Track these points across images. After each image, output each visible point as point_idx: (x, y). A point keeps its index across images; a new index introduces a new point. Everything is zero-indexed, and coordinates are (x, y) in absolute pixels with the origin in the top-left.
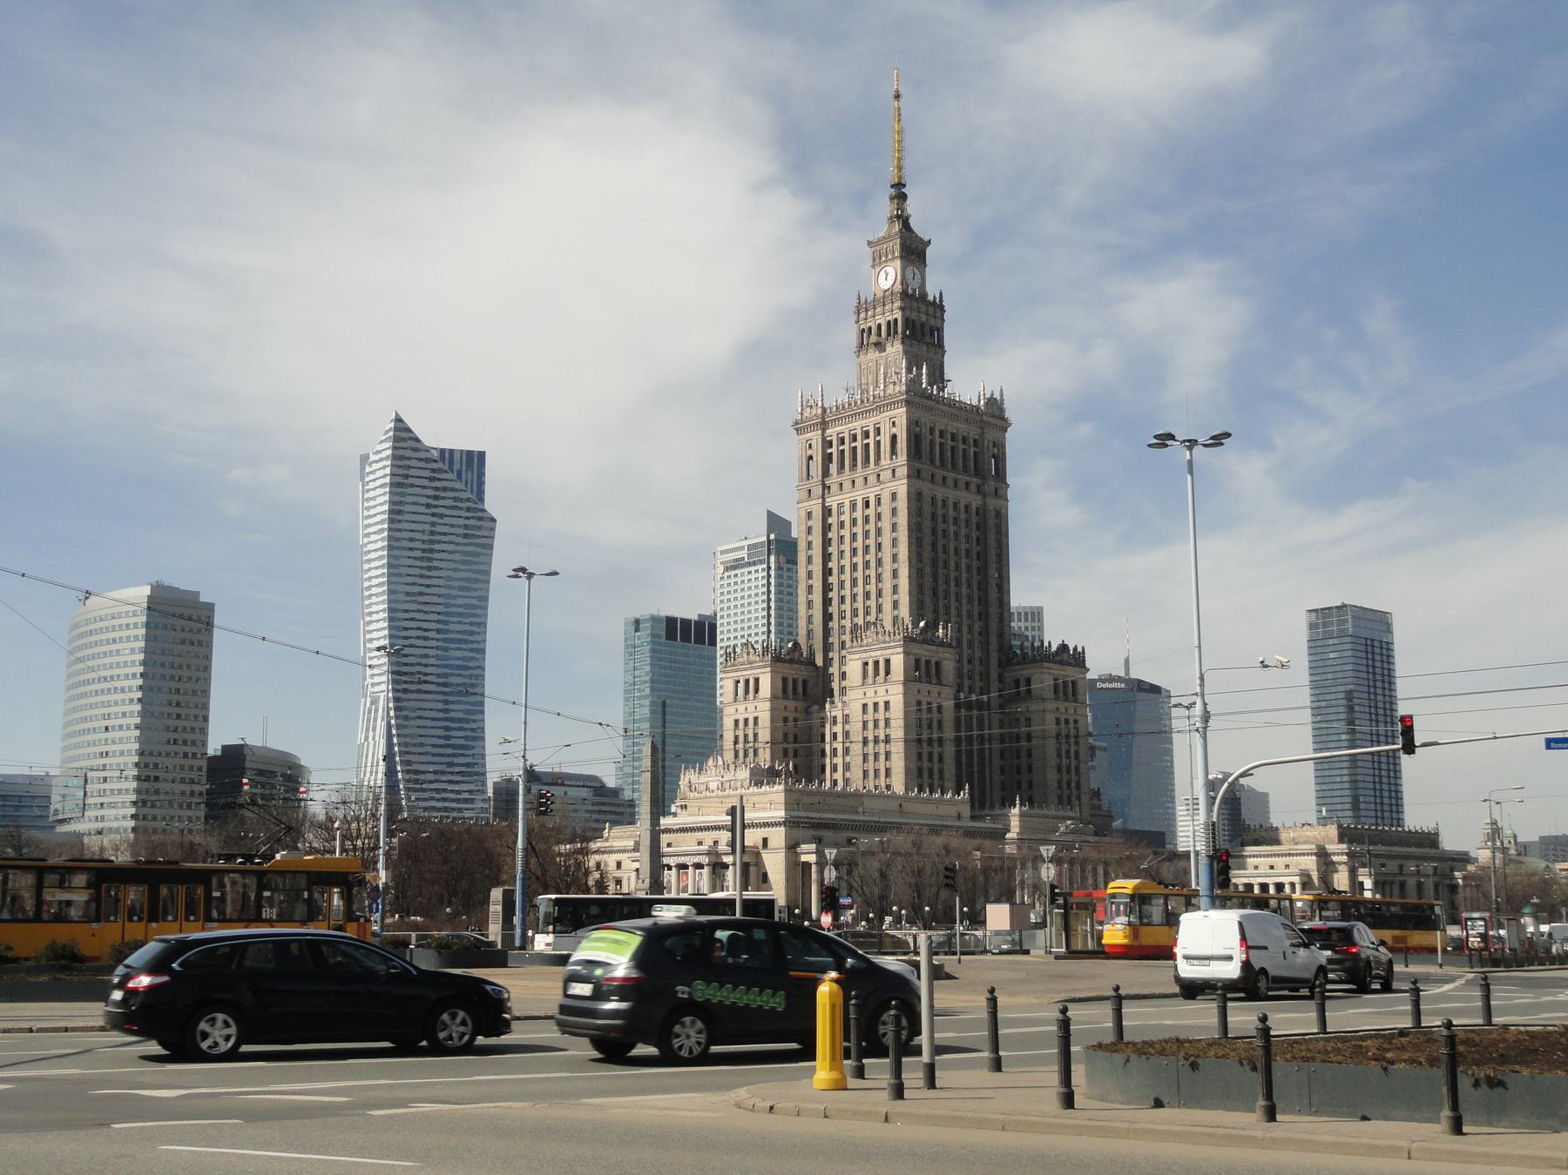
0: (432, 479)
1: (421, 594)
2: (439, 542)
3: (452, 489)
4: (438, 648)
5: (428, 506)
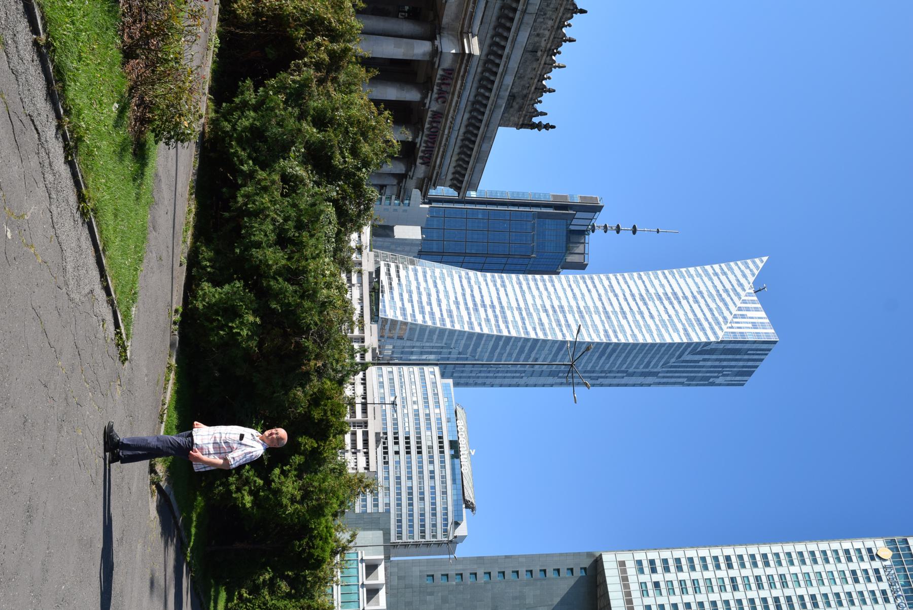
0: (726, 291)
1: (616, 295)
2: (671, 303)
3: (726, 304)
5: (701, 293)
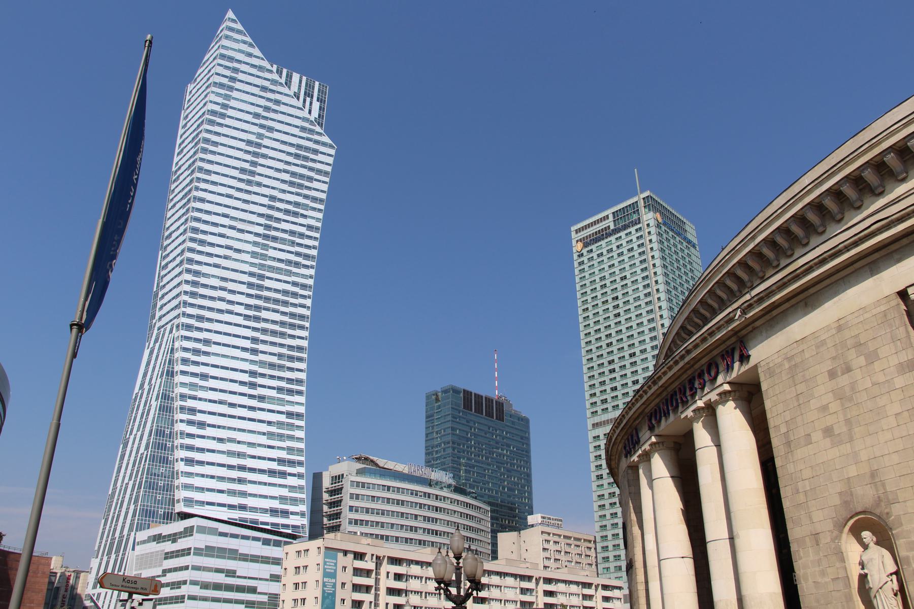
2: (264, 156)
4: (252, 274)
5: (257, 116)
